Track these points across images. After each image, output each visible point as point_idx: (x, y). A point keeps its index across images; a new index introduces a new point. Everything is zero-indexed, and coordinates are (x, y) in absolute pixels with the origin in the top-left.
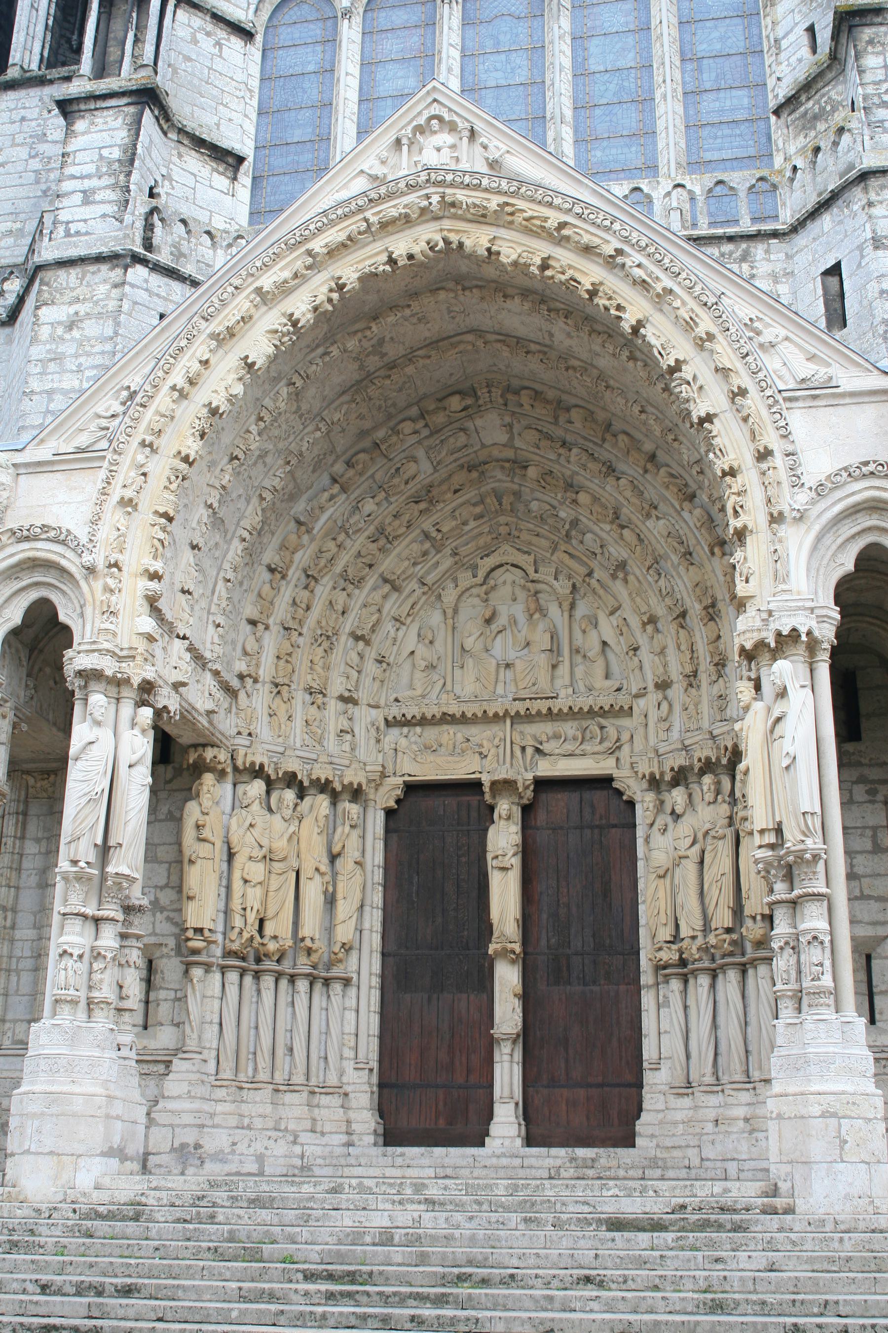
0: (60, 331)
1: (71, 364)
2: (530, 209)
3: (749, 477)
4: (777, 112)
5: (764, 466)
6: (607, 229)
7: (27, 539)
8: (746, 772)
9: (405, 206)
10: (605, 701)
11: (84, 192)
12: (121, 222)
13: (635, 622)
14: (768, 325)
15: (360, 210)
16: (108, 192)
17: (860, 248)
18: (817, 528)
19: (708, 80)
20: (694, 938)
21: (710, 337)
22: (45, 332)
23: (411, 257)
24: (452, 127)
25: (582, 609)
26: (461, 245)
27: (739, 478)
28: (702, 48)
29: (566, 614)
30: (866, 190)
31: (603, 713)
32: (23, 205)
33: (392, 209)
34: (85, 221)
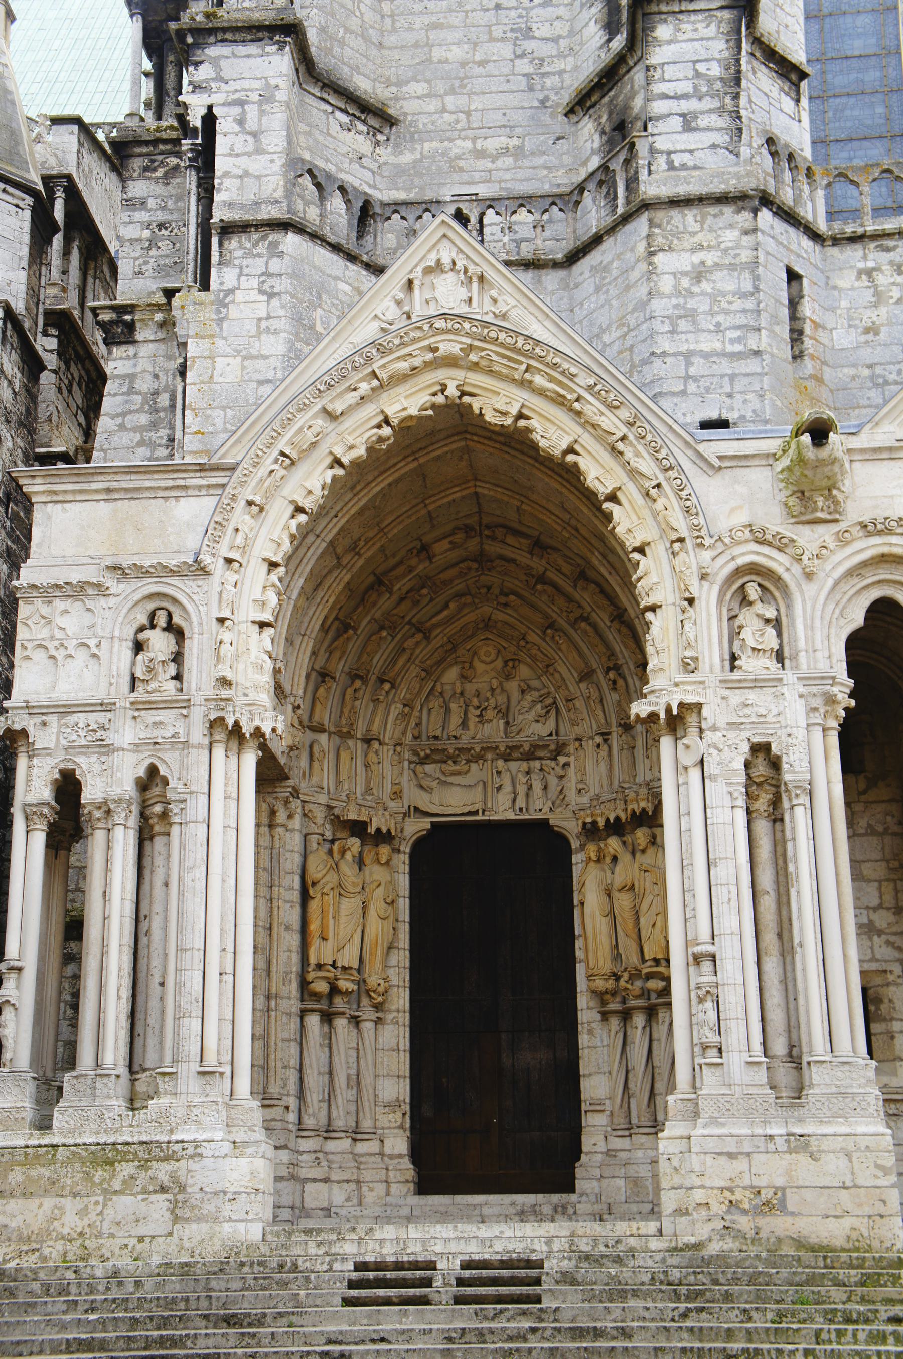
0: (685, 283)
1: (707, 323)
7: (880, 533)
11: (683, 116)
12: (737, 155)
16: (714, 117)
22: (666, 284)
32: (517, 117)
34: (691, 152)
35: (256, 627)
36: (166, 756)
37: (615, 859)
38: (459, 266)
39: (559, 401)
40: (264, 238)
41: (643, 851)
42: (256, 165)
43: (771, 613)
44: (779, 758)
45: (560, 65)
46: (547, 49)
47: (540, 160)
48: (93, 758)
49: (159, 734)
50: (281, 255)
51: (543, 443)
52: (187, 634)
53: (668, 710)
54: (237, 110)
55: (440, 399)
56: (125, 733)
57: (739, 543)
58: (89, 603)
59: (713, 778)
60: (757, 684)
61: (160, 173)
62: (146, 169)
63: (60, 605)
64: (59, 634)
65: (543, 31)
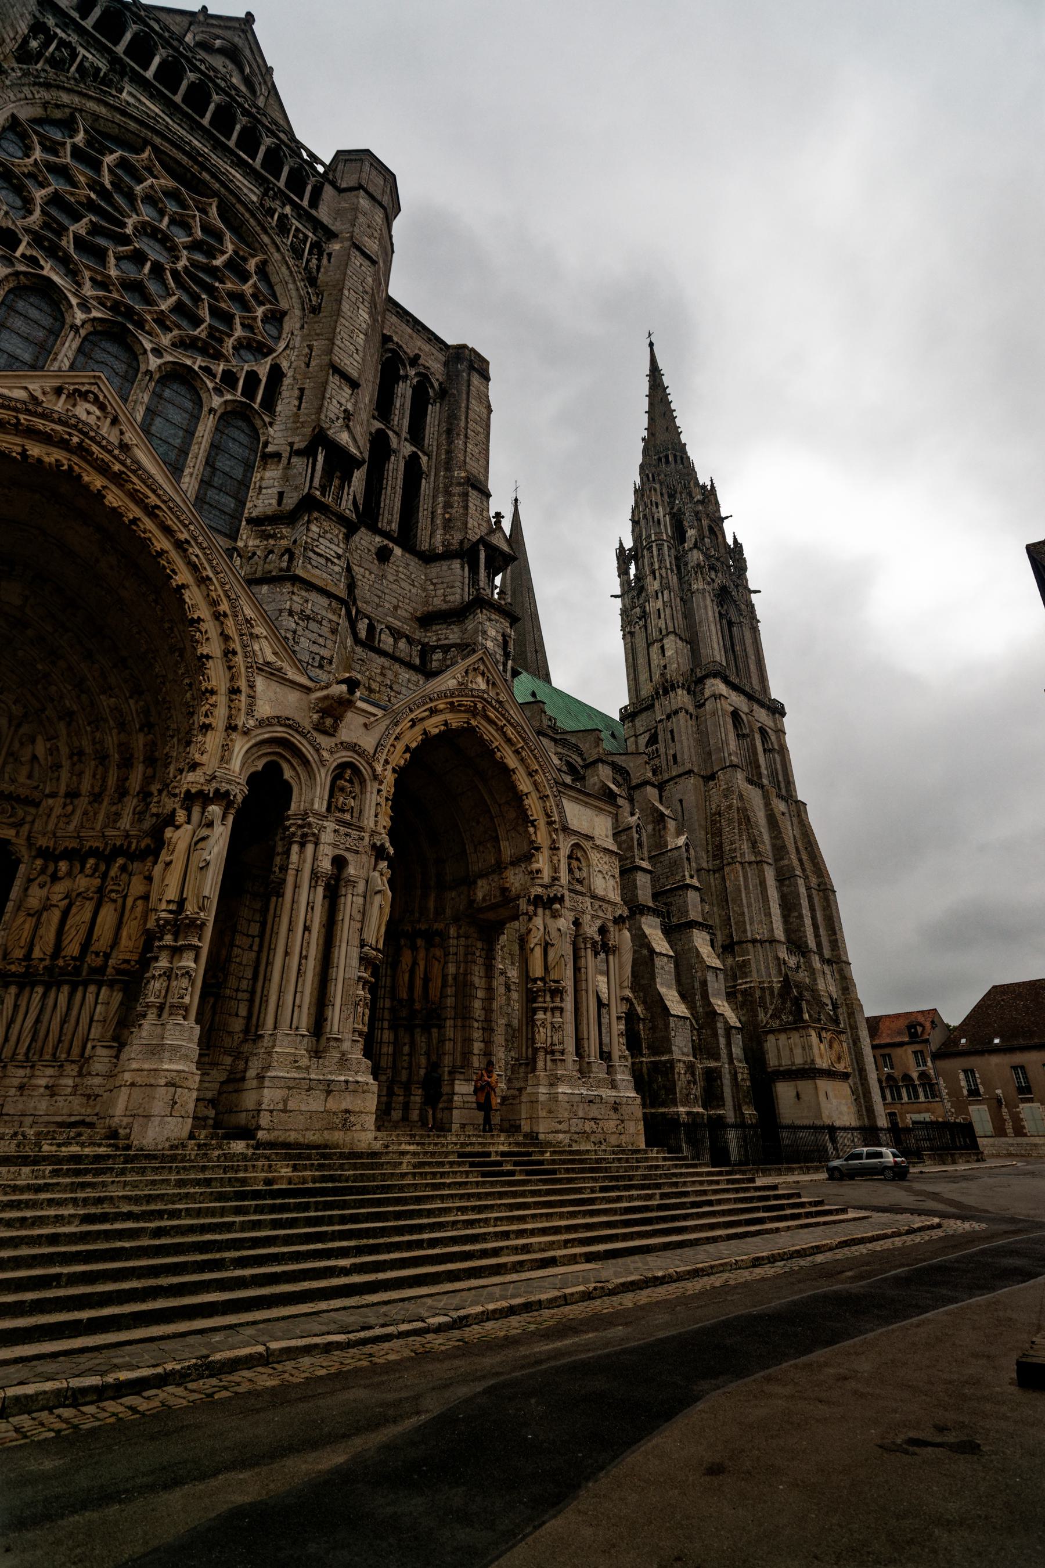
2: (139, 486)
3: (221, 700)
4: (249, 521)
5: (234, 697)
6: (185, 526)
8: (168, 864)
9: (52, 430)
10: (23, 792)
13: (64, 750)
14: (258, 625)
15: (15, 409)
17: (281, 611)
18: (253, 741)
19: (217, 481)
20: (42, 960)
21: (225, 615)
23: (39, 460)
24: (102, 407)
25: (25, 729)
26: (80, 476)
27: (214, 698)
28: (218, 465)
29: (13, 728)
30: (293, 585)
31: (18, 799)
33: (40, 424)
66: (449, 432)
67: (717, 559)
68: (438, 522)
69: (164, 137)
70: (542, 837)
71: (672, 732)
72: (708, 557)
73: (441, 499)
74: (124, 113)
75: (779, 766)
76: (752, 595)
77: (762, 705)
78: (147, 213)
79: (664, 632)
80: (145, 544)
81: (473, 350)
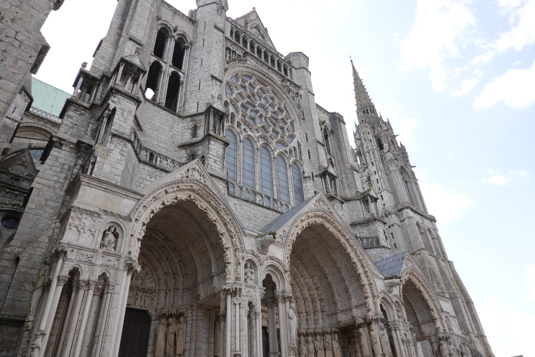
3: (367, 287)
24: (323, 201)
32: (168, 142)
35: (137, 240)
36: (110, 271)
37: (168, 325)
38: (200, 170)
39: (215, 209)
40: (123, 142)
41: (180, 323)
42: (124, 125)
43: (253, 271)
44: (253, 306)
45: (178, 137)
46: (176, 133)
47: (171, 153)
48: (86, 266)
49: (109, 263)
50: (127, 147)
51: (209, 217)
52: (120, 236)
53: (236, 288)
54: (122, 111)
55: (189, 198)
56: (99, 261)
57: (249, 253)
58: (94, 219)
59: (242, 308)
60: (251, 287)
61: (79, 113)
62: (75, 110)
63: (84, 216)
64: (82, 224)
65: (176, 129)
66: (339, 148)
67: (398, 155)
68: (346, 185)
69: (257, 71)
70: (436, 315)
71: (392, 233)
72: (394, 155)
73: (344, 176)
74: (248, 67)
75: (438, 245)
76: (413, 168)
77: (427, 218)
78: (263, 101)
79: (381, 189)
80: (339, 241)
81: (338, 114)
